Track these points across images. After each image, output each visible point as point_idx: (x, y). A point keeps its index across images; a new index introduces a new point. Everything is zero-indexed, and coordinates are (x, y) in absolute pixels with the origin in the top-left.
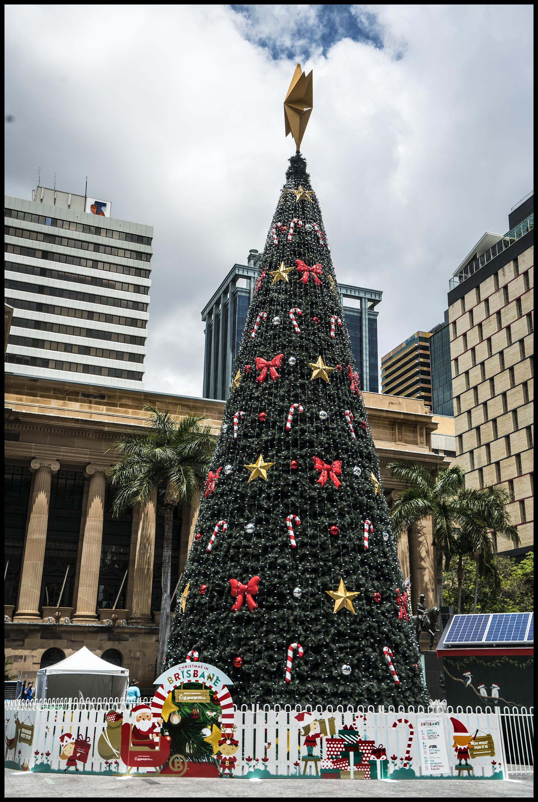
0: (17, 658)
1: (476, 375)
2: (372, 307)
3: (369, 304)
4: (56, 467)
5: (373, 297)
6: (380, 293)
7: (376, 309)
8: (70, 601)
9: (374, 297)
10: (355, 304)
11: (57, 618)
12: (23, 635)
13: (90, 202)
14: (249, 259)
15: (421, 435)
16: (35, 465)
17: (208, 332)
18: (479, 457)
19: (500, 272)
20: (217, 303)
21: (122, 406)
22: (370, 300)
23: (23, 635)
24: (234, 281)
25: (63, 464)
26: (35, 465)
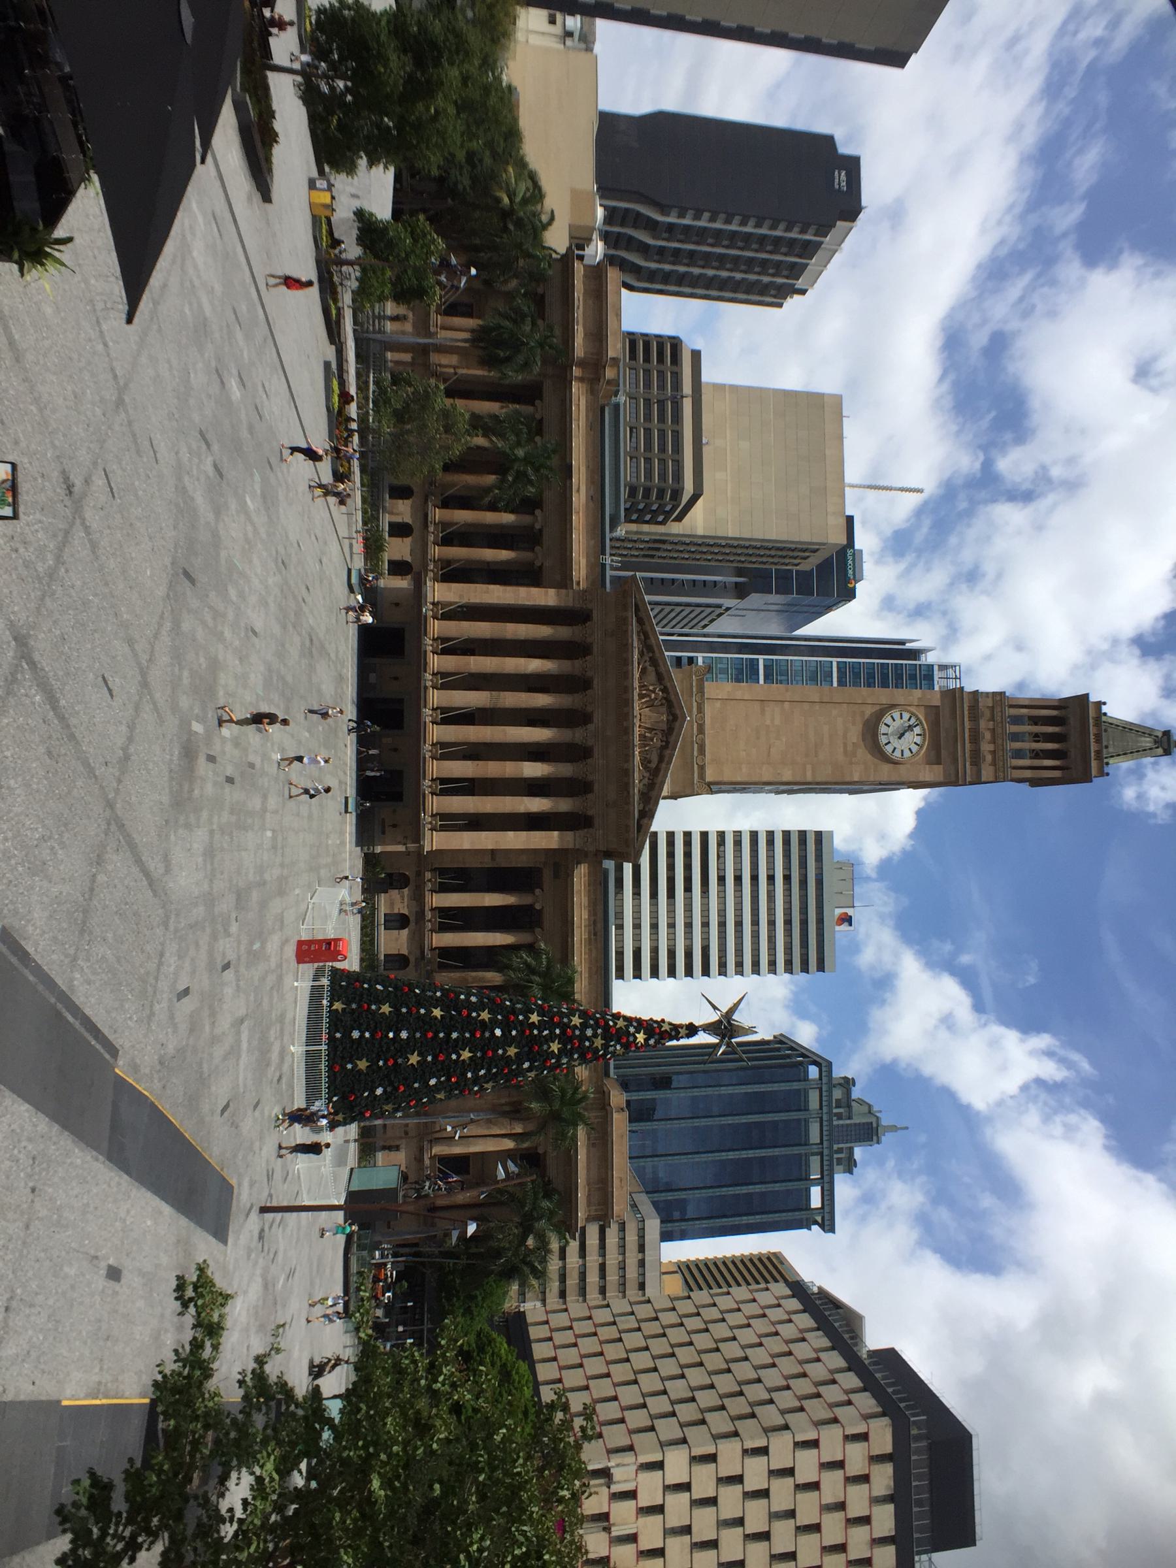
1: (713, 1313)
2: (816, 1223)
3: (819, 1219)
4: (538, 907)
5: (827, 1223)
7: (815, 1228)
8: (443, 928)
9: (828, 1225)
10: (816, 1201)
11: (430, 921)
12: (418, 898)
14: (846, 1079)
15: (596, 1210)
16: (537, 891)
18: (628, 1321)
19: (821, 1333)
20: (792, 1049)
21: (590, 950)
22: (823, 1219)
23: (418, 898)
25: (540, 912)
26: (537, 891)
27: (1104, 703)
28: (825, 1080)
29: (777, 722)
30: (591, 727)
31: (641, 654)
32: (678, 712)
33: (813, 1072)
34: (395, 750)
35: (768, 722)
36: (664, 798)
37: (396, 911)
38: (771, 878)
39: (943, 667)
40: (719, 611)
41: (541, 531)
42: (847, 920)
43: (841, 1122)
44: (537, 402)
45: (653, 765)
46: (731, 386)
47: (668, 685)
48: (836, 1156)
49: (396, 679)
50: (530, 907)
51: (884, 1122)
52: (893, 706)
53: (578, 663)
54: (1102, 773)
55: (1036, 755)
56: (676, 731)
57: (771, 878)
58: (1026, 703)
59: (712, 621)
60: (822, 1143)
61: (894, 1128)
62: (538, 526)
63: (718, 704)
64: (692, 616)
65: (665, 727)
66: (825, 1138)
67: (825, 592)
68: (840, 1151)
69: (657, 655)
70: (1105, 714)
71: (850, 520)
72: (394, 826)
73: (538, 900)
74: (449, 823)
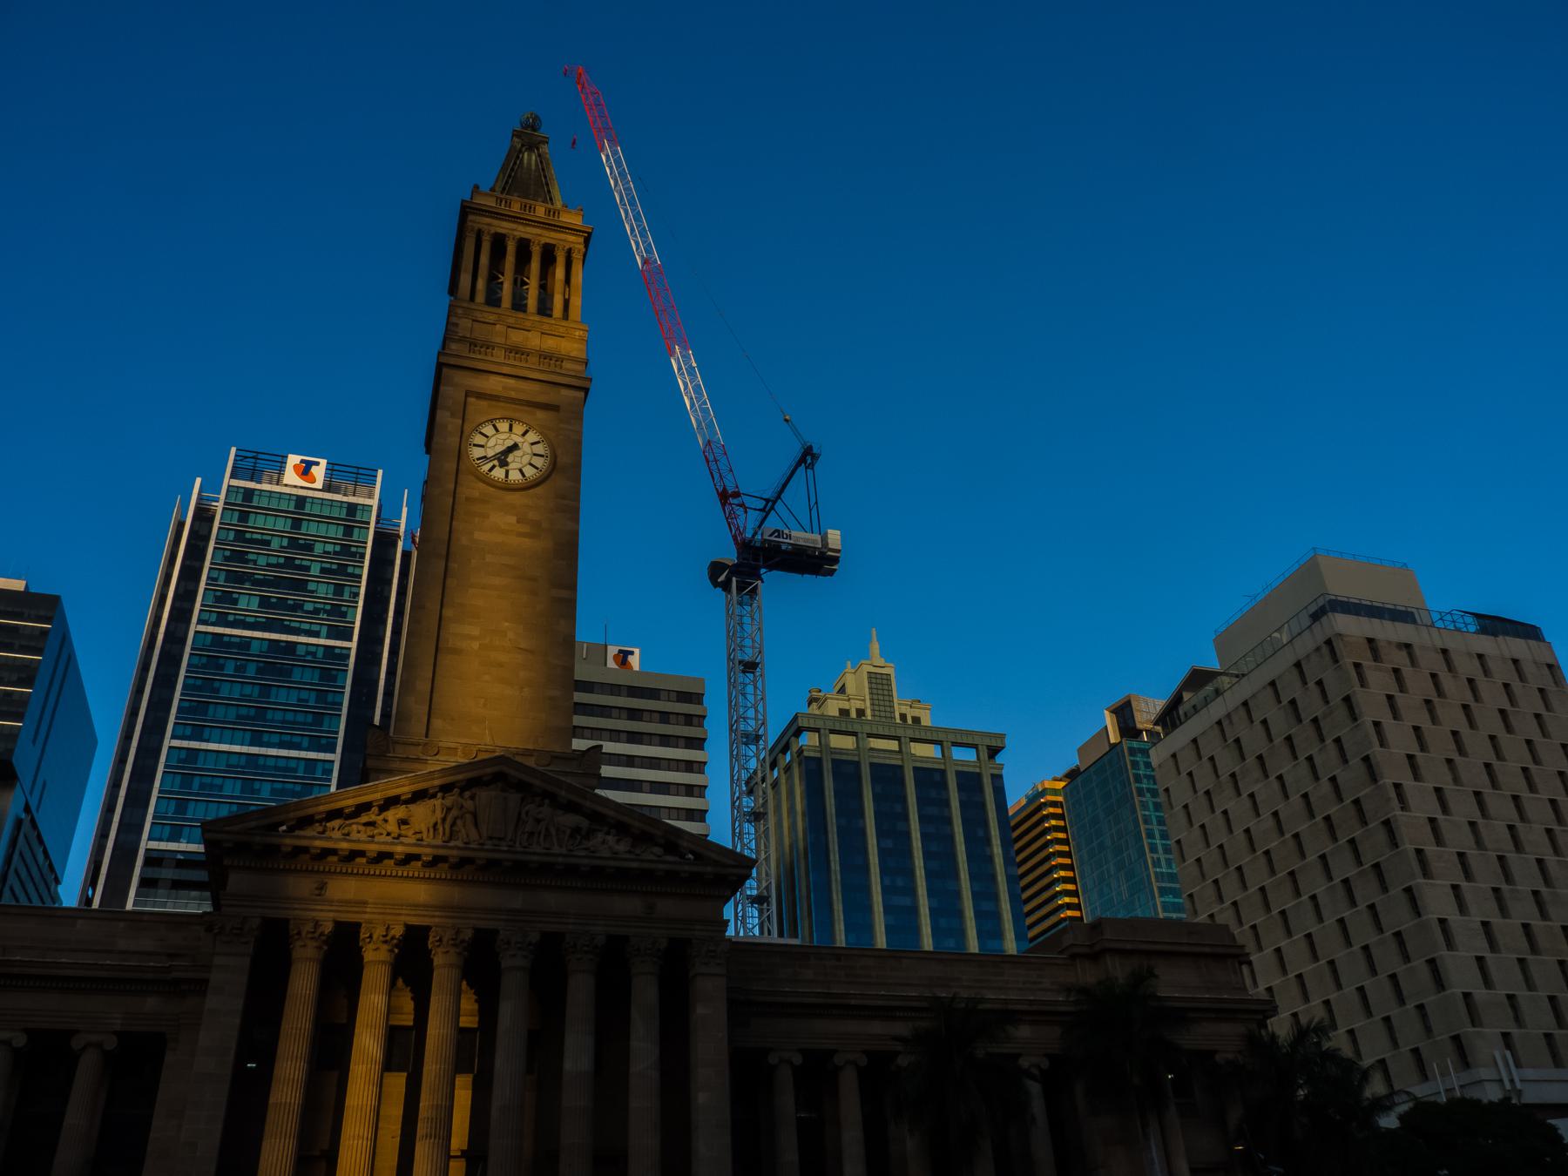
4: (798, 1060)
6: (1002, 736)
7: (999, 759)
10: (968, 755)
13: (612, 651)
16: (773, 1059)
26: (773, 1059)
29: (475, 631)
32: (489, 770)
35: (476, 645)
40: (26, 826)
45: (584, 823)
47: (437, 782)
52: (460, 455)
53: (369, 955)
59: (41, 842)
64: (24, 874)
70: (492, 190)
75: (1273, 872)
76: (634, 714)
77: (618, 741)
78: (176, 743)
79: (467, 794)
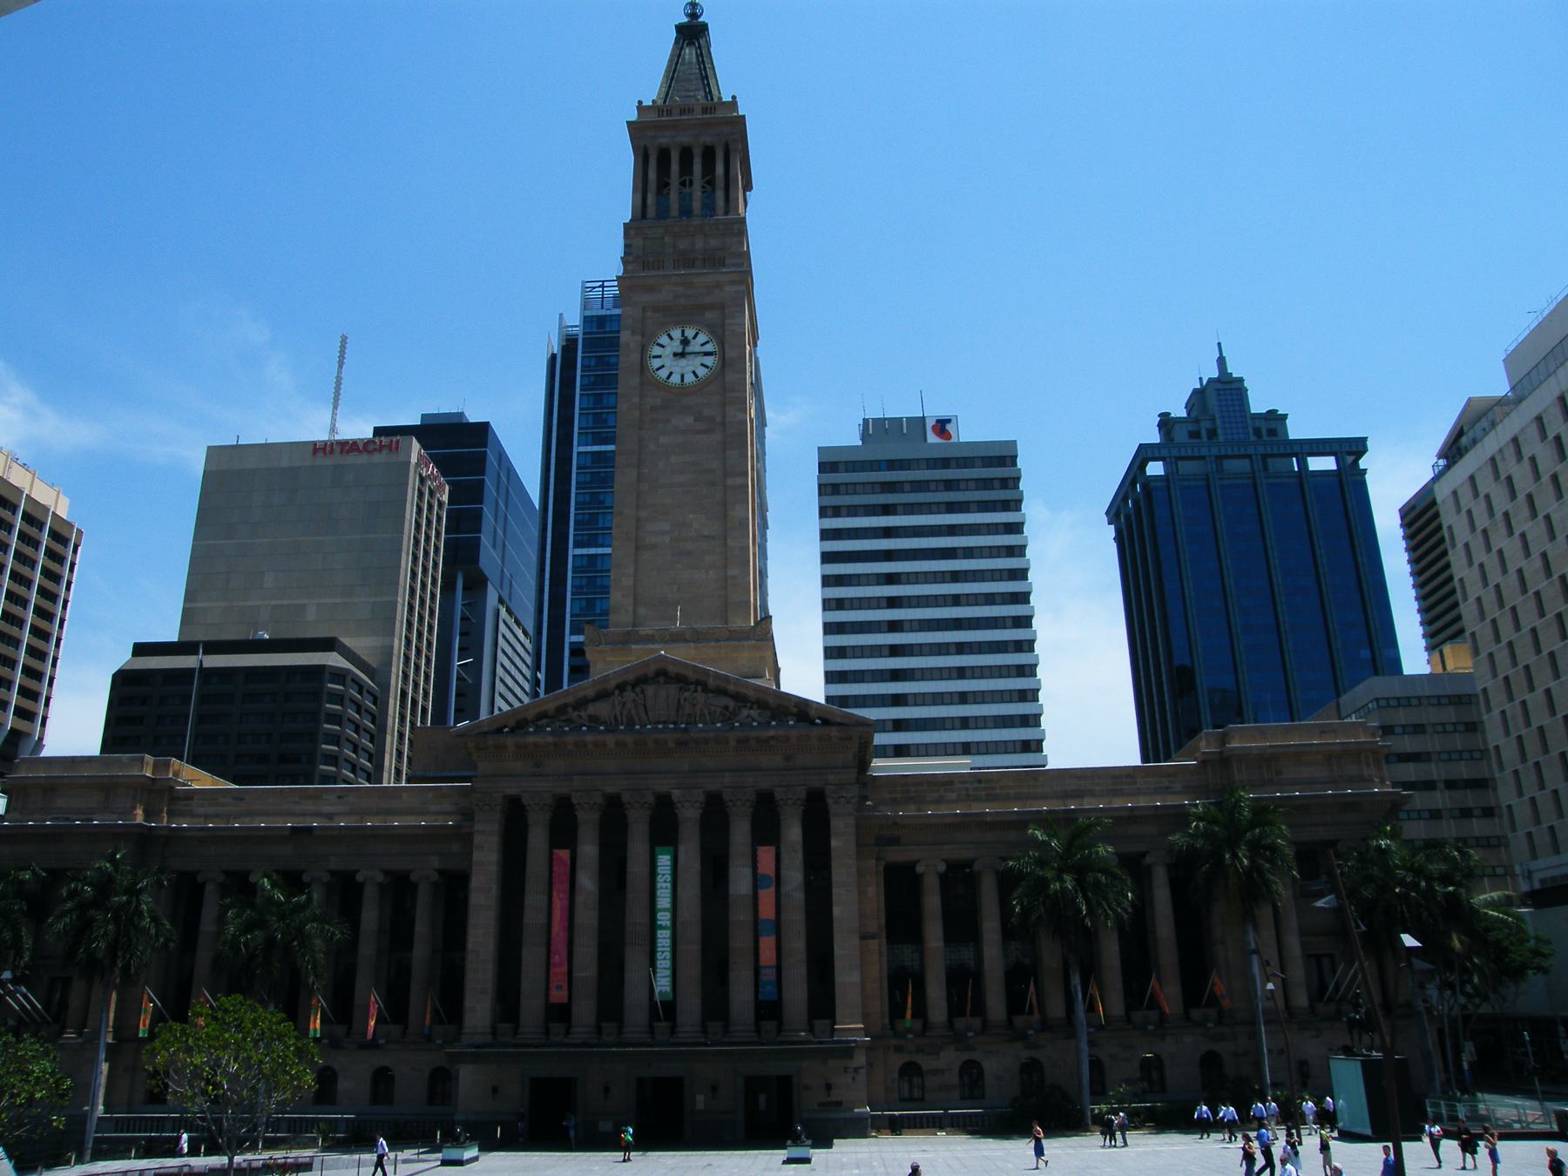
0: (935, 1072)
2: (1356, 462)
3: (1350, 459)
4: (942, 868)
6: (1364, 440)
7: (1362, 464)
9: (1357, 447)
17: (1119, 539)
22: (1350, 453)
24: (1142, 467)
27: (640, 102)
28: (1164, 453)
29: (666, 526)
30: (676, 794)
31: (569, 721)
32: (652, 669)
33: (1155, 469)
34: (714, 1089)
35: (667, 539)
36: (778, 685)
37: (955, 1080)
38: (888, 532)
39: (586, 303)
40: (503, 611)
41: (387, 873)
42: (942, 426)
43: (1219, 431)
44: (200, 878)
45: (731, 704)
46: (186, 600)
47: (613, 683)
48: (1265, 438)
49: (607, 1090)
50: (943, 878)
51: (1215, 375)
52: (643, 367)
53: (581, 815)
54: (733, 103)
55: (710, 182)
56: (683, 672)
57: (888, 532)
58: (639, 196)
60: (1249, 457)
61: (1221, 361)
62: (380, 877)
63: (642, 611)
65: (673, 689)
66: (1243, 452)
67: (477, 464)
68: (1257, 432)
69: (570, 699)
71: (379, 431)
72: (829, 1087)
73: (931, 868)
74: (823, 1003)
75: (1542, 614)
76: (949, 485)
77: (931, 513)
78: (579, 551)
79: (638, 689)
